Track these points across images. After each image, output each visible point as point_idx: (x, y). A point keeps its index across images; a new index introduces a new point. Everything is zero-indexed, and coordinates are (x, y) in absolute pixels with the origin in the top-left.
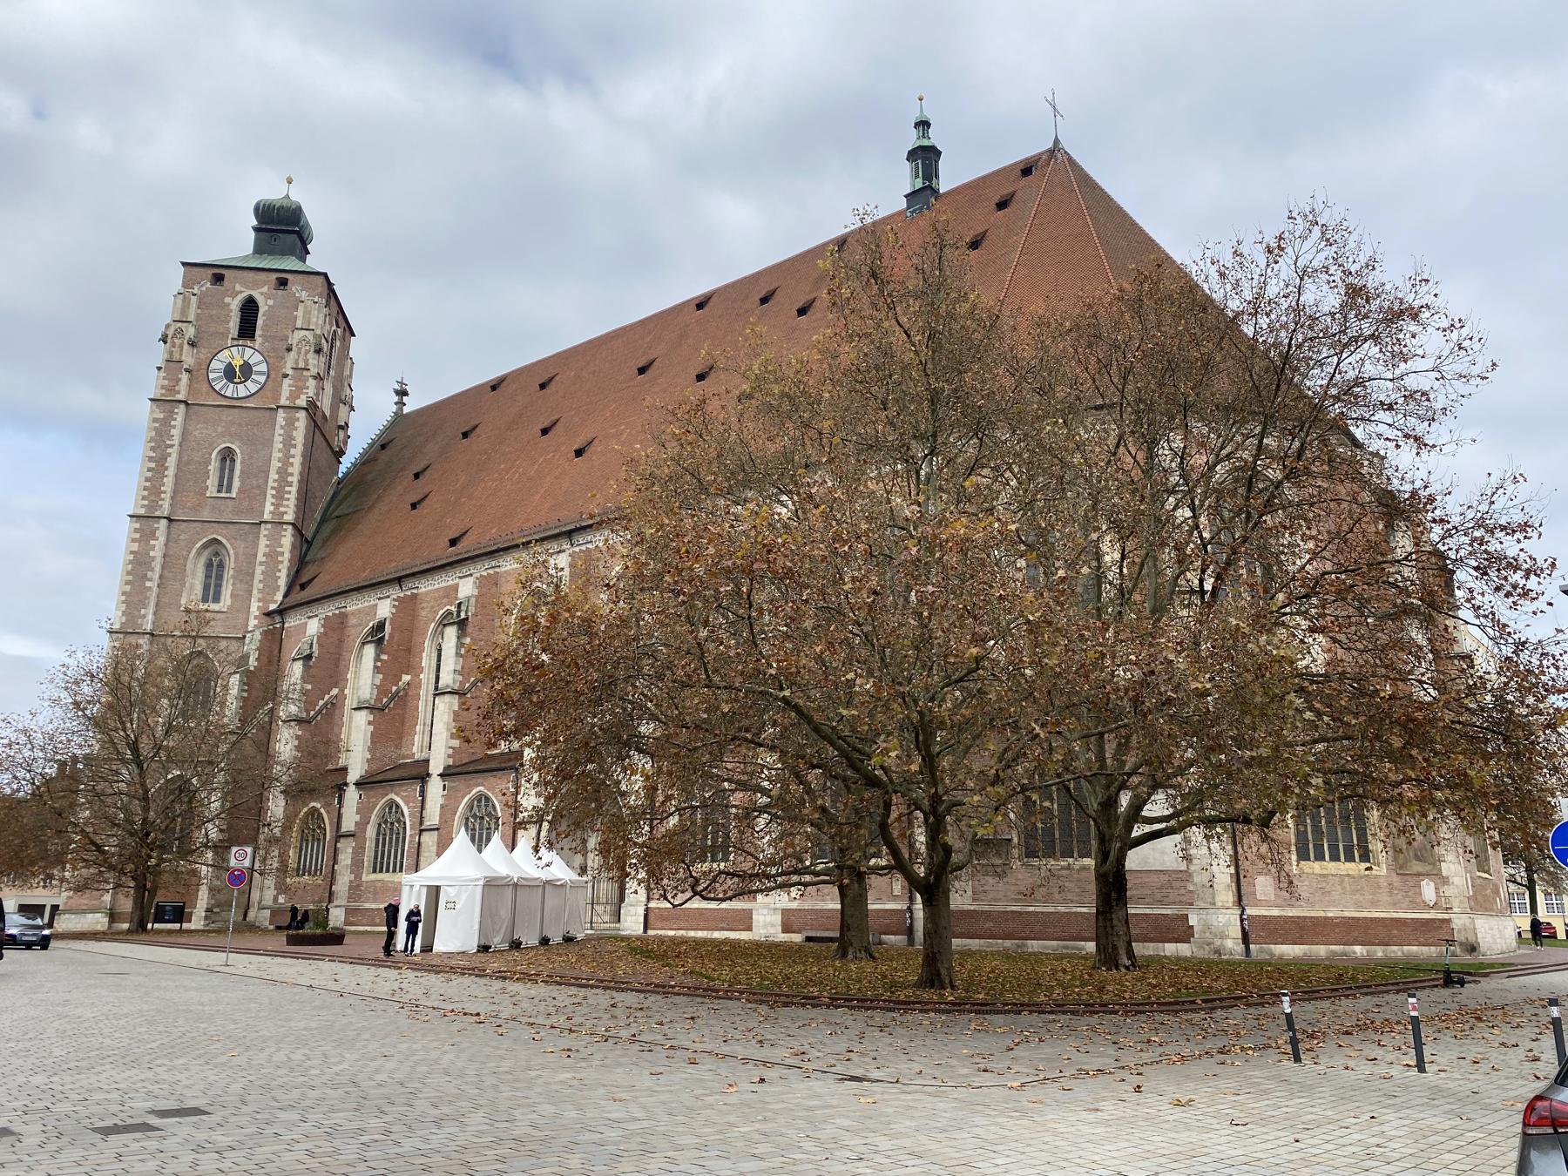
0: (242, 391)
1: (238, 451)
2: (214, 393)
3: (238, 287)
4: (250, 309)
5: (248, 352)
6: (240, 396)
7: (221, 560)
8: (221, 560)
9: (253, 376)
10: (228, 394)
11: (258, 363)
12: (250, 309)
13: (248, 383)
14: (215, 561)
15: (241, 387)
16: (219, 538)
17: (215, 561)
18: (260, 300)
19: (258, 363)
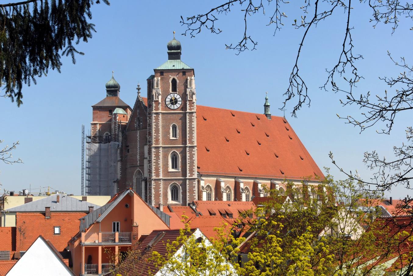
0: (176, 107)
1: (177, 125)
2: (168, 108)
3: (170, 76)
4: (174, 81)
5: (176, 95)
6: (175, 108)
7: (176, 157)
8: (176, 157)
9: (178, 102)
10: (172, 108)
11: (179, 98)
12: (174, 81)
13: (177, 104)
14: (174, 155)
15: (175, 106)
17: (174, 155)
18: (176, 78)
19: (179, 98)
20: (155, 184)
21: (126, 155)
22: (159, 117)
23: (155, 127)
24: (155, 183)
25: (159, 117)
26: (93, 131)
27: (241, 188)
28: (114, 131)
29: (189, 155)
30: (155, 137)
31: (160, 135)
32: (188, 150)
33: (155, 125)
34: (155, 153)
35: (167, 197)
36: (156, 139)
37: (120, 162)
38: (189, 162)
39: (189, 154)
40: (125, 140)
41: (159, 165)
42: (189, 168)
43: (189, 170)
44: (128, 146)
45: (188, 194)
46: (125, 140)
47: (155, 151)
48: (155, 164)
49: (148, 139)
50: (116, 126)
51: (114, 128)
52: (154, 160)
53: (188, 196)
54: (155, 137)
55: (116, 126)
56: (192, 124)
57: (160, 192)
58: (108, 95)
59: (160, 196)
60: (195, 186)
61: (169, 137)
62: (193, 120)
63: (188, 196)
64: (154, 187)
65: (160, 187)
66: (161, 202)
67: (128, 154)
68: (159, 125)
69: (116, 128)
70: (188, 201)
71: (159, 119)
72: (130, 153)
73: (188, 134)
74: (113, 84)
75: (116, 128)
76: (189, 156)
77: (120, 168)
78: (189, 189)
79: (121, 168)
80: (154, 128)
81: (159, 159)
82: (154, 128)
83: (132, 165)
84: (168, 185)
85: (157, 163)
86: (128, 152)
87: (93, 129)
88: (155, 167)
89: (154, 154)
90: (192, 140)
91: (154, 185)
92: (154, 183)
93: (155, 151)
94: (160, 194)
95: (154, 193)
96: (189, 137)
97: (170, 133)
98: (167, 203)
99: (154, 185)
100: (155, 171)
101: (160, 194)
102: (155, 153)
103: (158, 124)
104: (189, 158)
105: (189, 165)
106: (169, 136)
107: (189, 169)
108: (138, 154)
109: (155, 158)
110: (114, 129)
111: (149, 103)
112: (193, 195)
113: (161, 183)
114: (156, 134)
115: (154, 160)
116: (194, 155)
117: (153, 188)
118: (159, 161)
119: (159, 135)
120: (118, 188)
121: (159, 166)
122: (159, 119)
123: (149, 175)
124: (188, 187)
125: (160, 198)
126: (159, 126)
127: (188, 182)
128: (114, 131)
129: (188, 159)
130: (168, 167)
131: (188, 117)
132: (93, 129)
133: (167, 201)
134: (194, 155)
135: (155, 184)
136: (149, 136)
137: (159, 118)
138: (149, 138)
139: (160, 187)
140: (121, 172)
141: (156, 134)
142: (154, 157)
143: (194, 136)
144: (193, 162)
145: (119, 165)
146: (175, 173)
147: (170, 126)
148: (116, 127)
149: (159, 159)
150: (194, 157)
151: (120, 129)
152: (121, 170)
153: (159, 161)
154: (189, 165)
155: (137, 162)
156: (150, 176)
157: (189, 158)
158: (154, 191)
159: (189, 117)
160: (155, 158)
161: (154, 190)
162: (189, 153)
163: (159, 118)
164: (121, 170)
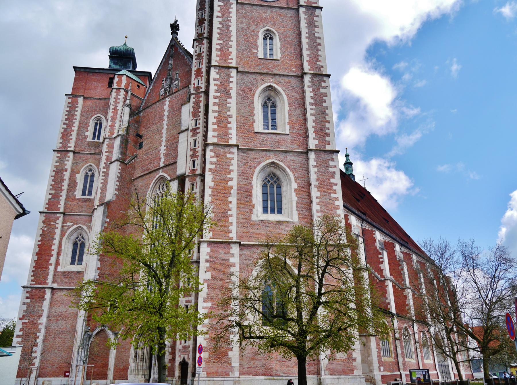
7: (273, 103)
8: (273, 103)
16: (272, 84)
20: (215, 160)
21: (135, 154)
22: (232, 8)
23: (221, 26)
24: (217, 156)
25: (232, 8)
26: (68, 109)
27: (379, 241)
28: (113, 105)
29: (312, 95)
30: (218, 47)
31: (233, 43)
32: (310, 84)
33: (220, 23)
34: (218, 83)
35: (251, 201)
36: (222, 51)
37: (119, 163)
38: (313, 112)
39: (311, 92)
40: (136, 125)
41: (229, 111)
42: (314, 125)
43: (313, 129)
44: (141, 137)
45: (315, 193)
46: (136, 125)
47: (218, 76)
48: (216, 108)
49: (194, 84)
50: (119, 97)
51: (114, 100)
52: (215, 97)
53: (317, 198)
54: (218, 47)
55: (119, 97)
56: (314, 30)
57: (230, 183)
58: (112, 64)
59: (230, 195)
60: (334, 172)
61: (257, 53)
62: (316, 24)
63: (317, 198)
64: (213, 166)
65: (231, 168)
66: (307, 68)
67: (138, 151)
68: (230, 24)
69: (118, 101)
70: (317, 212)
71: (231, 12)
72: (145, 147)
73: (307, 49)
74: (124, 50)
75: (118, 101)
76: (312, 98)
77: (118, 177)
78: (318, 180)
79: (119, 175)
80: (218, 28)
81: (230, 98)
82: (218, 28)
83: (148, 169)
84: (255, 167)
85: (223, 106)
86: (141, 146)
87: (70, 105)
88: (216, 114)
89: (215, 85)
90: (318, 63)
91: (211, 163)
92: (211, 157)
93: (218, 76)
94: (232, 187)
95: (212, 184)
96: (308, 55)
97: (257, 46)
98: (250, 217)
99: (211, 163)
100: (216, 126)
101: (232, 187)
102: (218, 83)
103: (230, 21)
104: (312, 101)
105: (313, 118)
106: (256, 51)
107: (313, 127)
108: (164, 143)
109: (218, 94)
110: (114, 102)
111: (200, 17)
112: (330, 197)
113: (233, 159)
114: (221, 42)
115: (215, 97)
116: (326, 96)
117: (210, 170)
118: (230, 103)
119: (230, 43)
120: (107, 218)
121: (228, 113)
122: (231, 12)
123: (192, 163)
124: (316, 173)
125: (230, 199)
126: (230, 26)
127: (315, 160)
128: (113, 105)
129: (311, 104)
130: (254, 122)
131: (303, 16)
132: (68, 107)
133: (251, 212)
134: (326, 96)
135: (215, 160)
136: (196, 77)
137: (230, 10)
138: (196, 82)
139: (231, 168)
140: (118, 184)
141: (221, 42)
142: (216, 91)
143: (321, 56)
144: (325, 112)
145: (115, 169)
146: (274, 136)
147: (258, 32)
148: (119, 99)
149: (230, 98)
150: (325, 101)
151: (128, 101)
152: (117, 181)
153: (230, 103)
154: (313, 118)
155: (160, 159)
156: (194, 167)
157: (312, 101)
158: (213, 180)
159: (306, 17)
160: (218, 94)
161: (212, 177)
162: (311, 89)
163: (230, 10)
164: (117, 181)
